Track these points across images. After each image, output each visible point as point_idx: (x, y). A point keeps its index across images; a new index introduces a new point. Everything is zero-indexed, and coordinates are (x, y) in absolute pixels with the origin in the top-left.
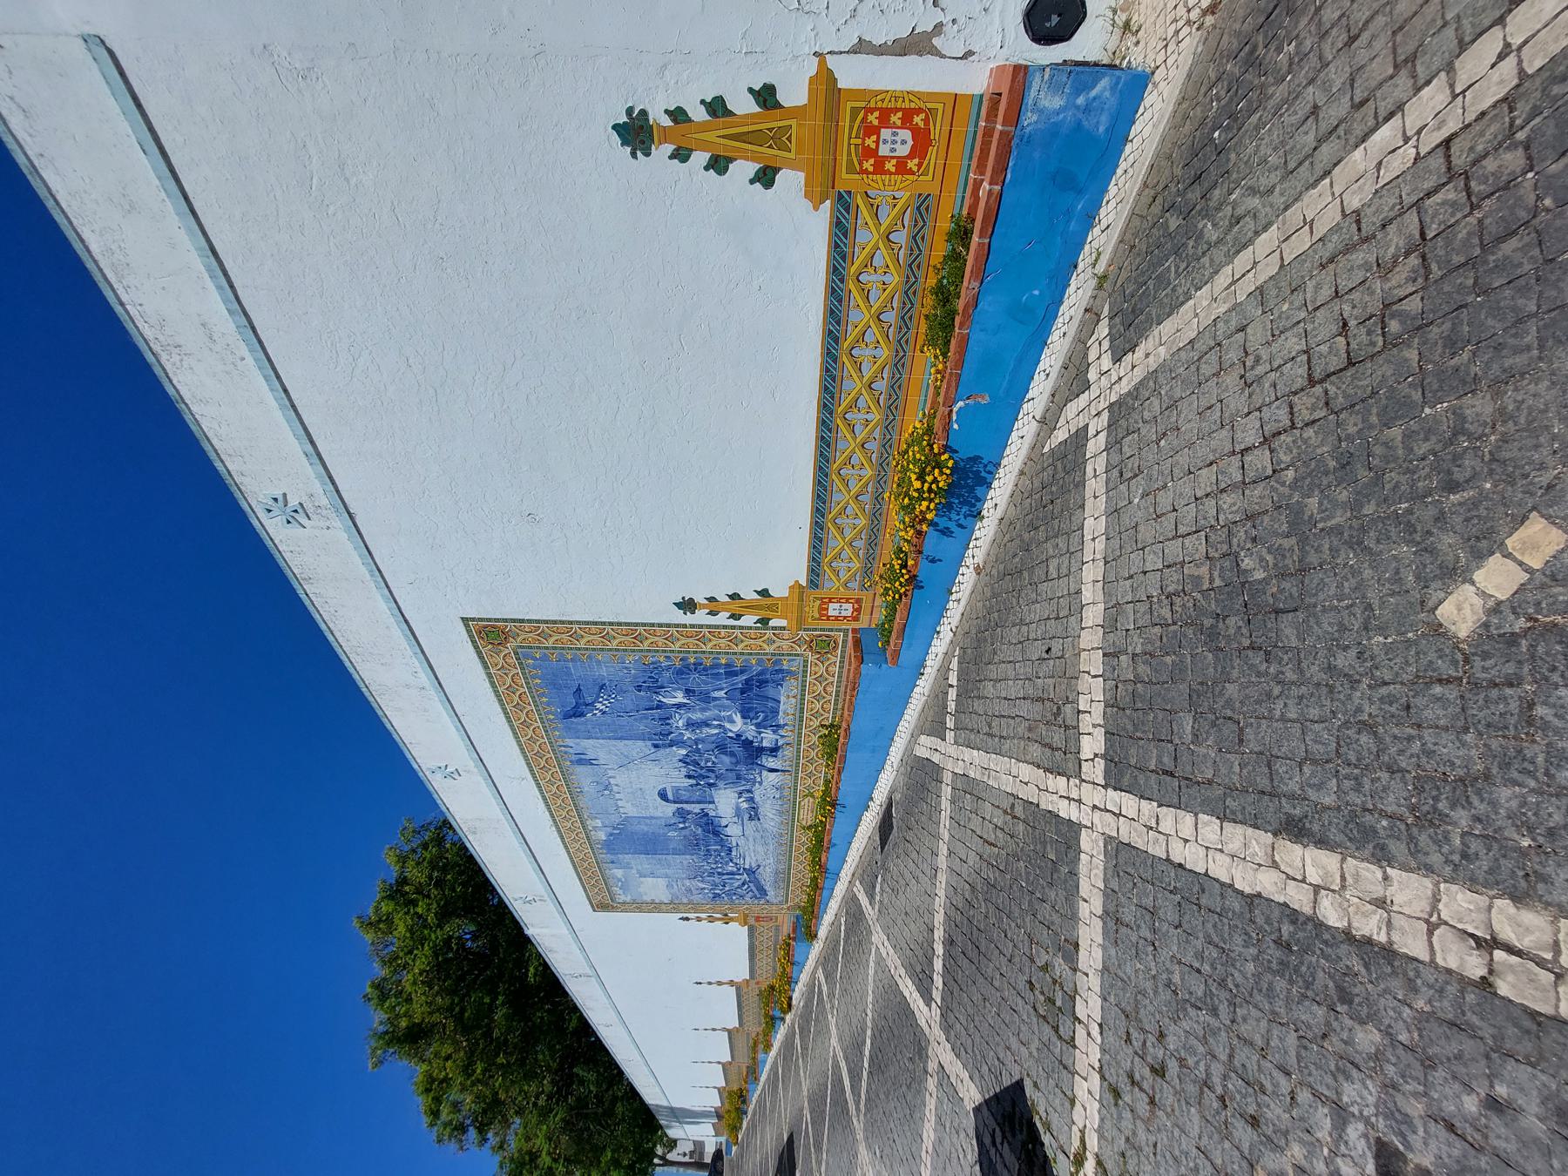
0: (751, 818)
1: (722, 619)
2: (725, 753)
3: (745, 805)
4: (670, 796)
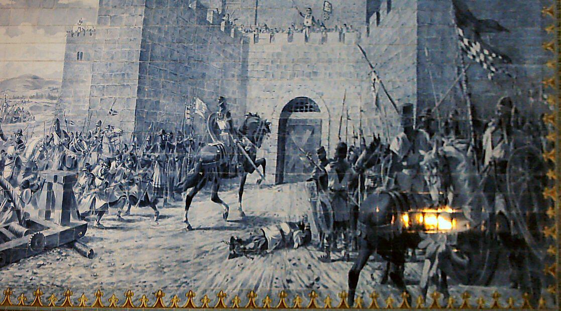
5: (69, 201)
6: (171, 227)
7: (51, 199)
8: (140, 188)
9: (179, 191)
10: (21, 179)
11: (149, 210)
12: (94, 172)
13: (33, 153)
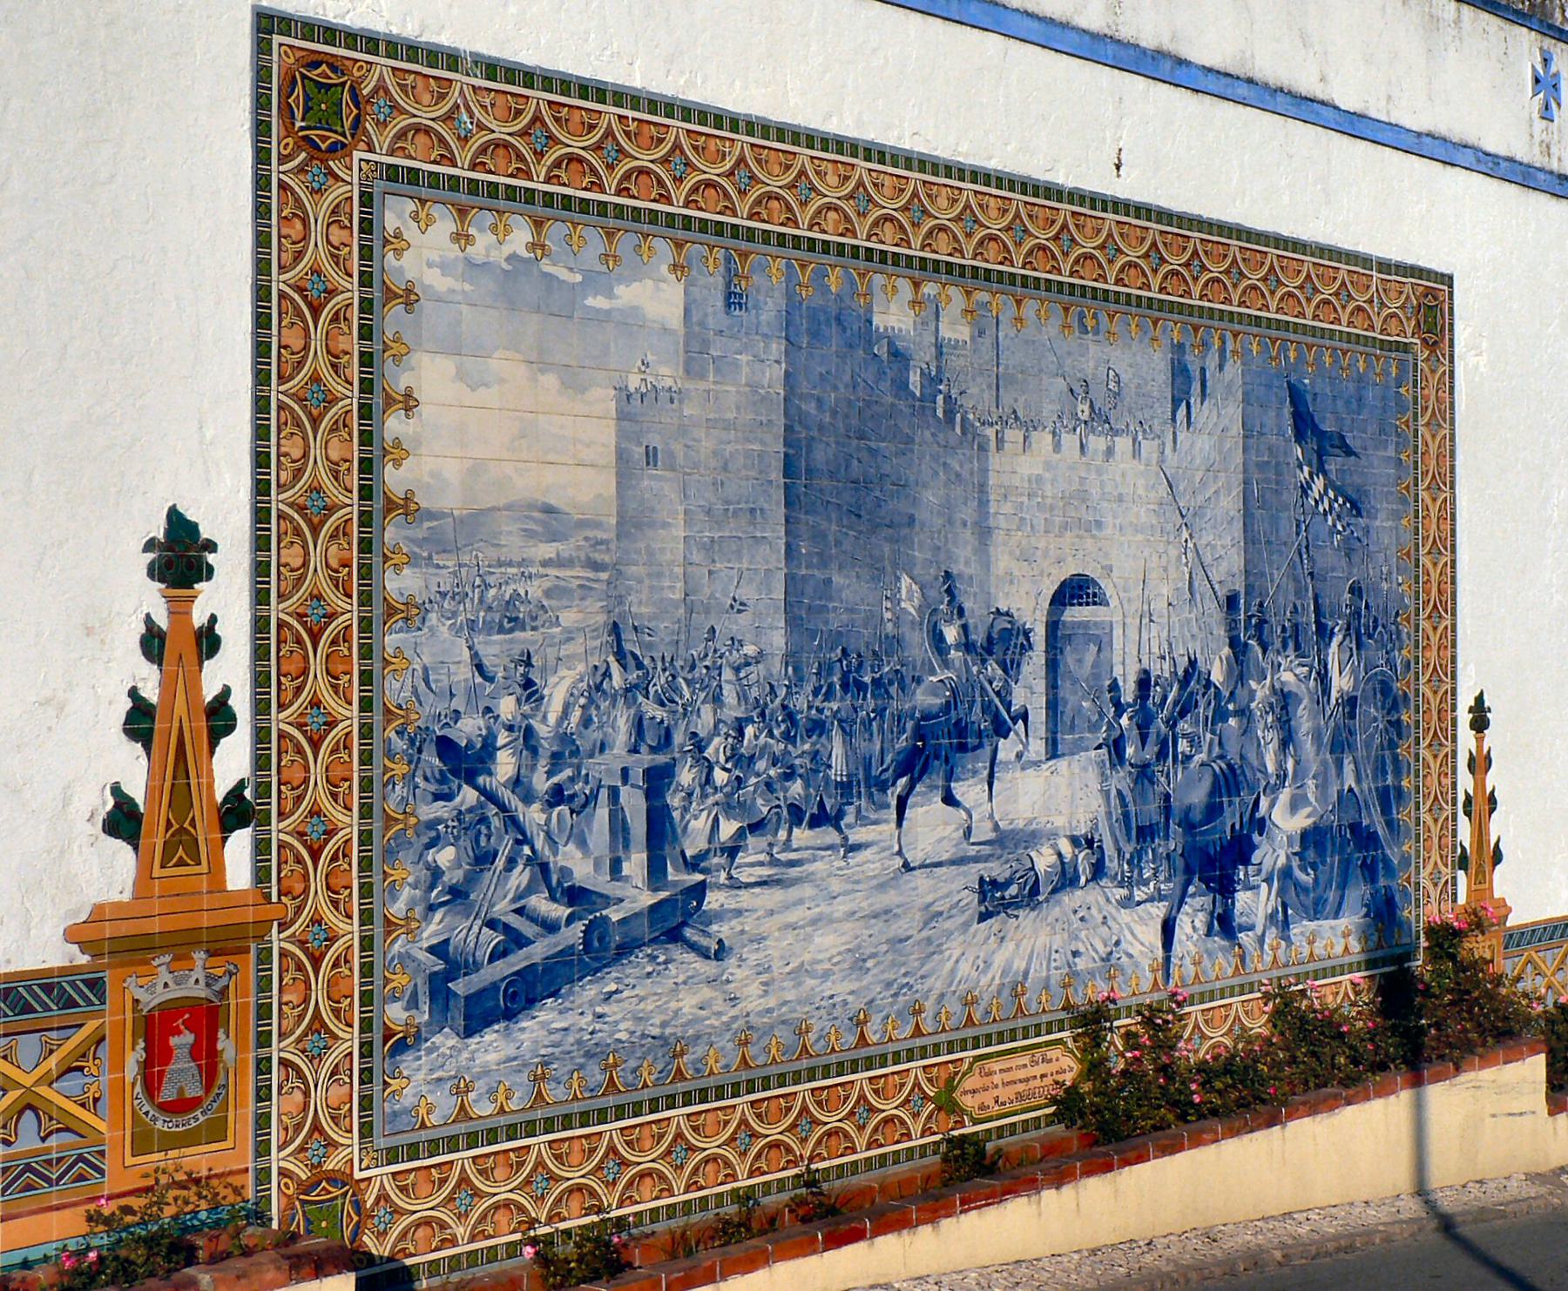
0: (988, 888)
2: (1215, 790)
3: (1044, 861)
4: (1074, 614)
5: (660, 829)
6: (873, 868)
7: (619, 829)
8: (807, 786)
9: (883, 787)
10: (541, 783)
11: (829, 835)
12: (709, 752)
13: (565, 713)
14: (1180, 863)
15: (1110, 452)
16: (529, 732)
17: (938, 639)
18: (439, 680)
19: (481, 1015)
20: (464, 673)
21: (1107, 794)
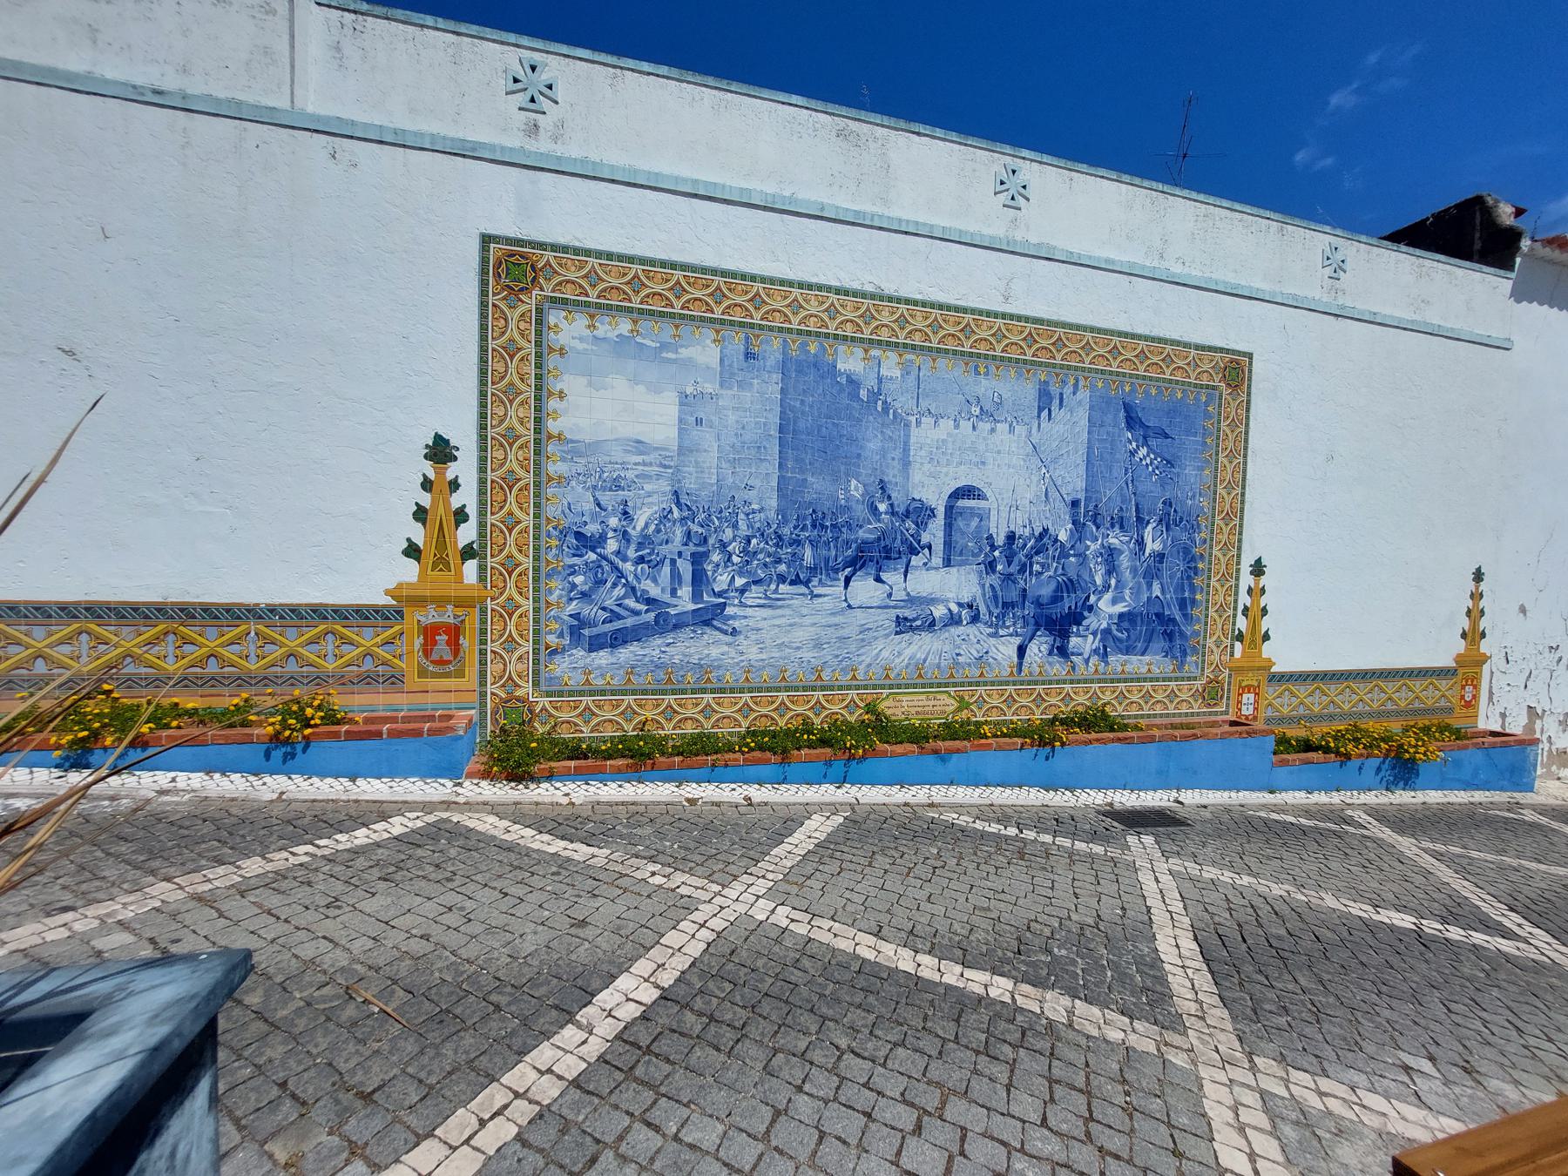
0: (899, 621)
1: (1244, 599)
2: (1059, 588)
3: (939, 612)
5: (699, 579)
6: (830, 606)
7: (676, 577)
8: (789, 567)
9: (836, 571)
10: (631, 553)
11: (803, 589)
12: (730, 548)
13: (647, 525)
14: (1032, 621)
15: (993, 430)
16: (625, 532)
17: (874, 510)
18: (577, 508)
19: (595, 645)
20: (588, 506)
21: (983, 586)
